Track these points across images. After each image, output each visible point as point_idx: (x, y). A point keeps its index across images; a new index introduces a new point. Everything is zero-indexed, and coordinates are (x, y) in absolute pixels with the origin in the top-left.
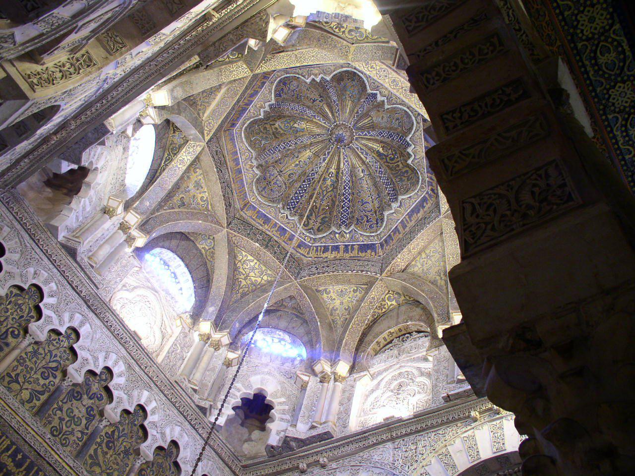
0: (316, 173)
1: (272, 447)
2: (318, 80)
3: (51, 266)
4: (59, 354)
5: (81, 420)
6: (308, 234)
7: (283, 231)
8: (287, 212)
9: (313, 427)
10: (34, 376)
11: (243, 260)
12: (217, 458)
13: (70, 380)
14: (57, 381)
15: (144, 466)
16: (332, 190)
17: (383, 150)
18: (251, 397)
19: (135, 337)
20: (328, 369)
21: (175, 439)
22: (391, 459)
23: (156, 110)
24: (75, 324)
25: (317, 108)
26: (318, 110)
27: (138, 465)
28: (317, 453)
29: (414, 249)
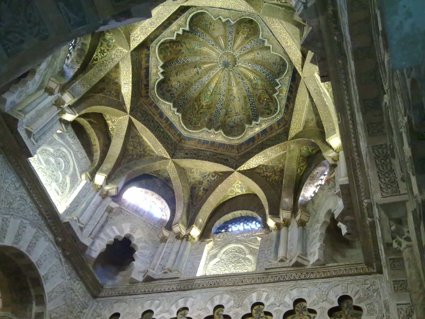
0: (249, 89)
1: (347, 234)
2: (162, 70)
3: (150, 295)
6: (275, 115)
7: (264, 132)
8: (254, 123)
11: (265, 170)
12: (344, 278)
16: (264, 81)
17: (244, 34)
20: (332, 154)
23: (109, 184)
25: (203, 72)
26: (205, 72)
29: (287, 43)
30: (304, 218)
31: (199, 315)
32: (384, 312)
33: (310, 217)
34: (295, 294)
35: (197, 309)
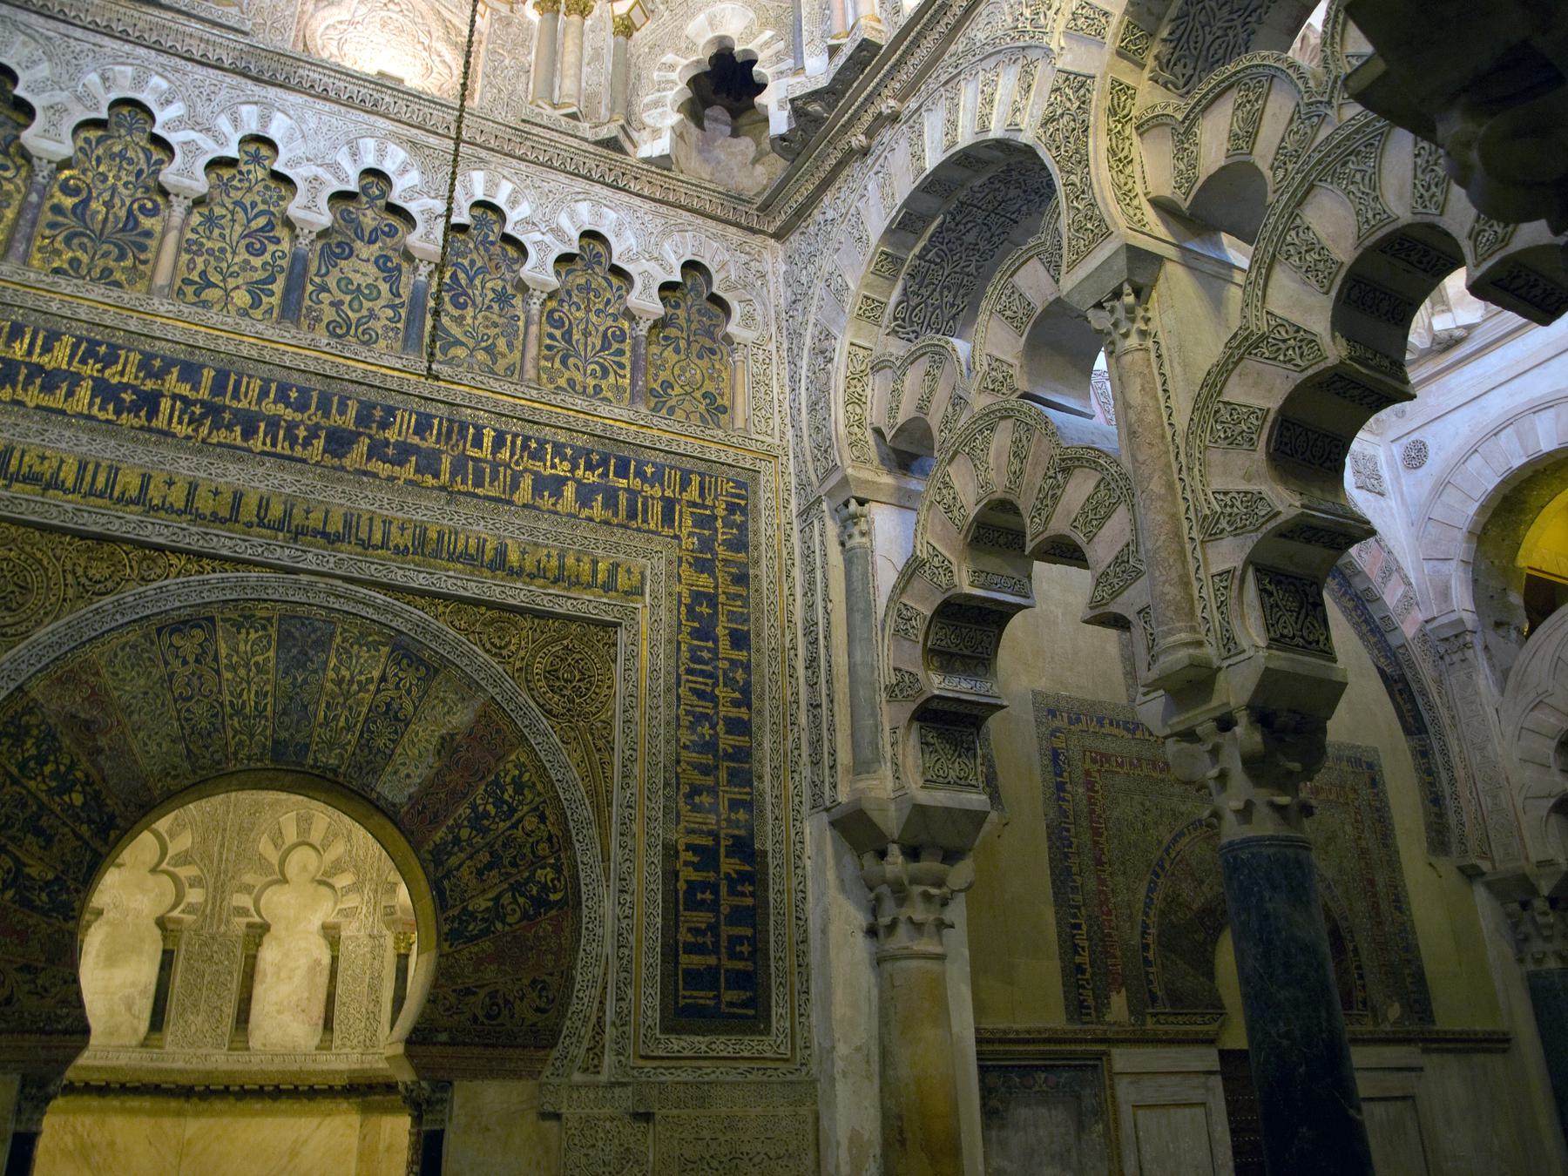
1: (782, 138)
3: (127, 47)
4: (258, 199)
5: (376, 287)
9: (833, 51)
10: (237, 260)
12: (699, 220)
13: (306, 231)
14: (285, 245)
15: (552, 304)
18: (708, 68)
19: (383, 82)
21: (587, 227)
22: (1009, 20)
24: (253, 127)
27: (535, 308)
28: (870, 99)
30: (637, 16)
31: (316, 179)
32: (773, 329)
33: (648, 18)
34: (585, 215)
35: (308, 160)
